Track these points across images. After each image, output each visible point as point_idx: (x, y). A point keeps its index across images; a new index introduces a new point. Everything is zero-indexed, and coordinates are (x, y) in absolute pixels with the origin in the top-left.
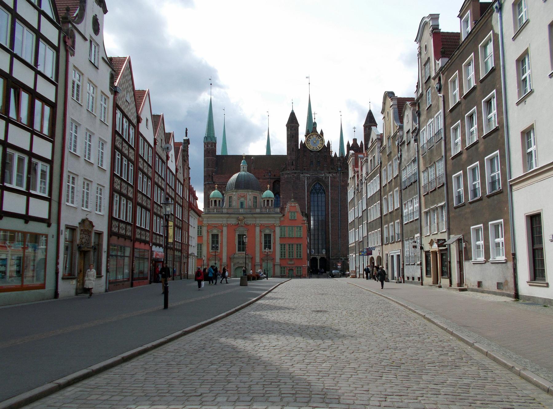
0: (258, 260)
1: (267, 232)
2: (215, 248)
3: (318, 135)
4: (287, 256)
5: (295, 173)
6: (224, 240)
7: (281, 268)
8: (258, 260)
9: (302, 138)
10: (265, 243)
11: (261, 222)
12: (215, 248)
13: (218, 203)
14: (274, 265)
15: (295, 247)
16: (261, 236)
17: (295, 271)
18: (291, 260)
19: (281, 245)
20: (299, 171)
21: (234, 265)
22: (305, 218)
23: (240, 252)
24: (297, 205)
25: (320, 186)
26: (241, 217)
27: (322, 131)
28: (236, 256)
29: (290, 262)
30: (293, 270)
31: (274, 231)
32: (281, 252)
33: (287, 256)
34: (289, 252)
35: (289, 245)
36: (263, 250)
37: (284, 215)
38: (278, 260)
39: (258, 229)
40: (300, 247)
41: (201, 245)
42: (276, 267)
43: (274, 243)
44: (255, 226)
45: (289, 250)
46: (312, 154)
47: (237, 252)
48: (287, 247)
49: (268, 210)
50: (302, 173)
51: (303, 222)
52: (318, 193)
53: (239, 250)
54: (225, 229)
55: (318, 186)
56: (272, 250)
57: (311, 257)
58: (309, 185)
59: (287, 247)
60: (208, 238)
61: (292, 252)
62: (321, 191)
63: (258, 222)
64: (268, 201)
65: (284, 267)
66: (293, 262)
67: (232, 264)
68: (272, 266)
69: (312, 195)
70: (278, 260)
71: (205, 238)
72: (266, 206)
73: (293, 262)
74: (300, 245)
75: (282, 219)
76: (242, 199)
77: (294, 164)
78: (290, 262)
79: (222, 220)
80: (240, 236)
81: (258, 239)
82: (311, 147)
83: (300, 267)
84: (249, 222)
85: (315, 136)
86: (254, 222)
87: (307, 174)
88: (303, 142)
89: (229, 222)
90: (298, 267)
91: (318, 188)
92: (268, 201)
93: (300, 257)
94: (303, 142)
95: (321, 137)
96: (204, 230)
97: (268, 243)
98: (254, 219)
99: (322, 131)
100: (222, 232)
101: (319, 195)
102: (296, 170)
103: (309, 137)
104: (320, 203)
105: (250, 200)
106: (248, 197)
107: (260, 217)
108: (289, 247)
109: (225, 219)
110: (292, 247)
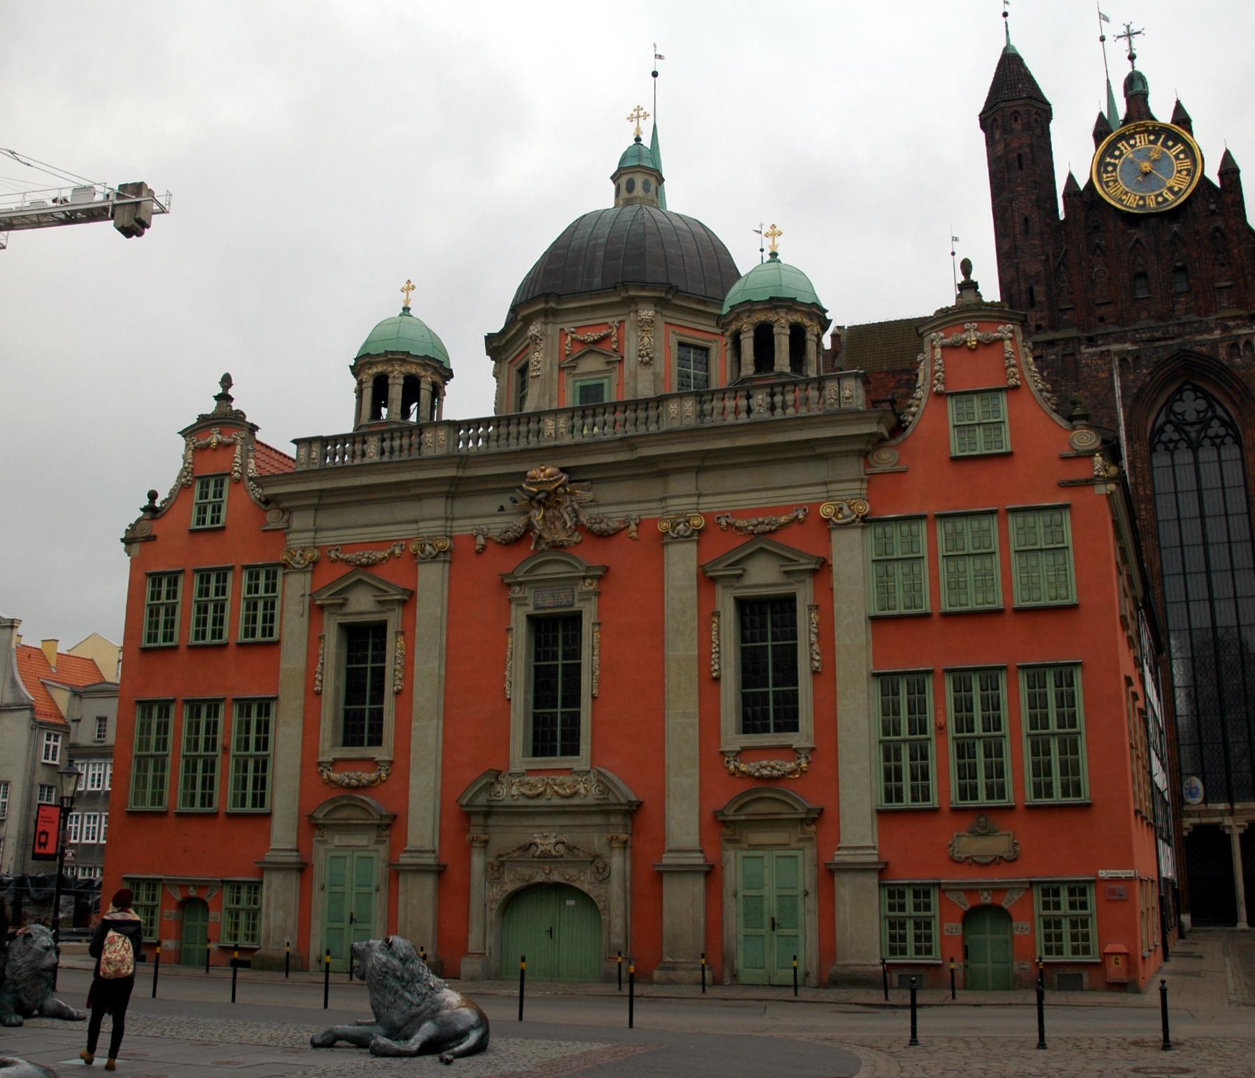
0: (683, 824)
1: (763, 576)
2: (361, 724)
3: (1159, 131)
4: (944, 786)
5: (1051, 343)
6: (421, 665)
7: (895, 894)
8: (683, 824)
9: (1072, 156)
10: (751, 670)
11: (711, 504)
12: (361, 724)
13: (396, 392)
14: (829, 873)
15: (1014, 698)
16: (707, 616)
17: (1028, 925)
18: (983, 819)
19: (886, 681)
20: (1073, 333)
21: (497, 868)
22: (1085, 439)
23: (541, 762)
24: (1005, 330)
25: (1201, 404)
26: (543, 472)
27: (1179, 108)
28: (508, 792)
29: (970, 846)
30: (1001, 914)
31: (822, 570)
32: (890, 752)
33: (944, 786)
34: (964, 750)
35: (961, 678)
36: (732, 737)
37: (898, 428)
38: (858, 828)
39: (681, 564)
40: (1066, 700)
41: (265, 706)
42: (845, 888)
43: (825, 675)
44: (663, 540)
45: (964, 724)
46: (1137, 234)
47: (518, 756)
48: (941, 705)
49: (760, 398)
50: (1091, 341)
51: (1078, 471)
52: (1194, 446)
53: (542, 744)
54: (431, 581)
55: (1190, 406)
56: (802, 738)
57: (1188, 822)
58: (1135, 401)
59: (941, 705)
60: (313, 657)
61: (994, 750)
62: (1216, 428)
63: (676, 505)
64: (764, 336)
65: (922, 892)
66: (997, 845)
67: (478, 862)
68: (805, 876)
69: (1161, 460)
70: (858, 828)
71: (293, 658)
72: (748, 370)
73: (997, 845)
74: (1065, 674)
75: (886, 458)
76: (592, 364)
77: (1040, 297)
78: (970, 846)
79: (407, 511)
80: (554, 633)
81: (681, 649)
82: (1124, 196)
83: (1078, 890)
84: (613, 516)
85: (1141, 141)
86: (651, 511)
87: (1122, 340)
88: (1082, 183)
89: (463, 527)
90: (1050, 890)
91: (1190, 417)
92: (764, 336)
93: (1073, 788)
94: (1082, 183)
95: (1178, 139)
96: (294, 592)
97: (769, 674)
98: (654, 488)
99: (1179, 108)
100: (408, 600)
101: (1208, 454)
102: (1054, 327)
103: (1112, 146)
104: (1213, 502)
105: (646, 362)
106: (632, 345)
107: (702, 464)
108: (964, 705)
109: (436, 507)
110: (992, 704)
